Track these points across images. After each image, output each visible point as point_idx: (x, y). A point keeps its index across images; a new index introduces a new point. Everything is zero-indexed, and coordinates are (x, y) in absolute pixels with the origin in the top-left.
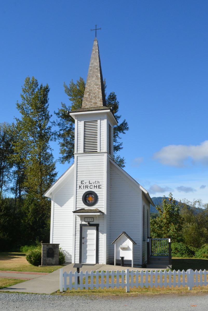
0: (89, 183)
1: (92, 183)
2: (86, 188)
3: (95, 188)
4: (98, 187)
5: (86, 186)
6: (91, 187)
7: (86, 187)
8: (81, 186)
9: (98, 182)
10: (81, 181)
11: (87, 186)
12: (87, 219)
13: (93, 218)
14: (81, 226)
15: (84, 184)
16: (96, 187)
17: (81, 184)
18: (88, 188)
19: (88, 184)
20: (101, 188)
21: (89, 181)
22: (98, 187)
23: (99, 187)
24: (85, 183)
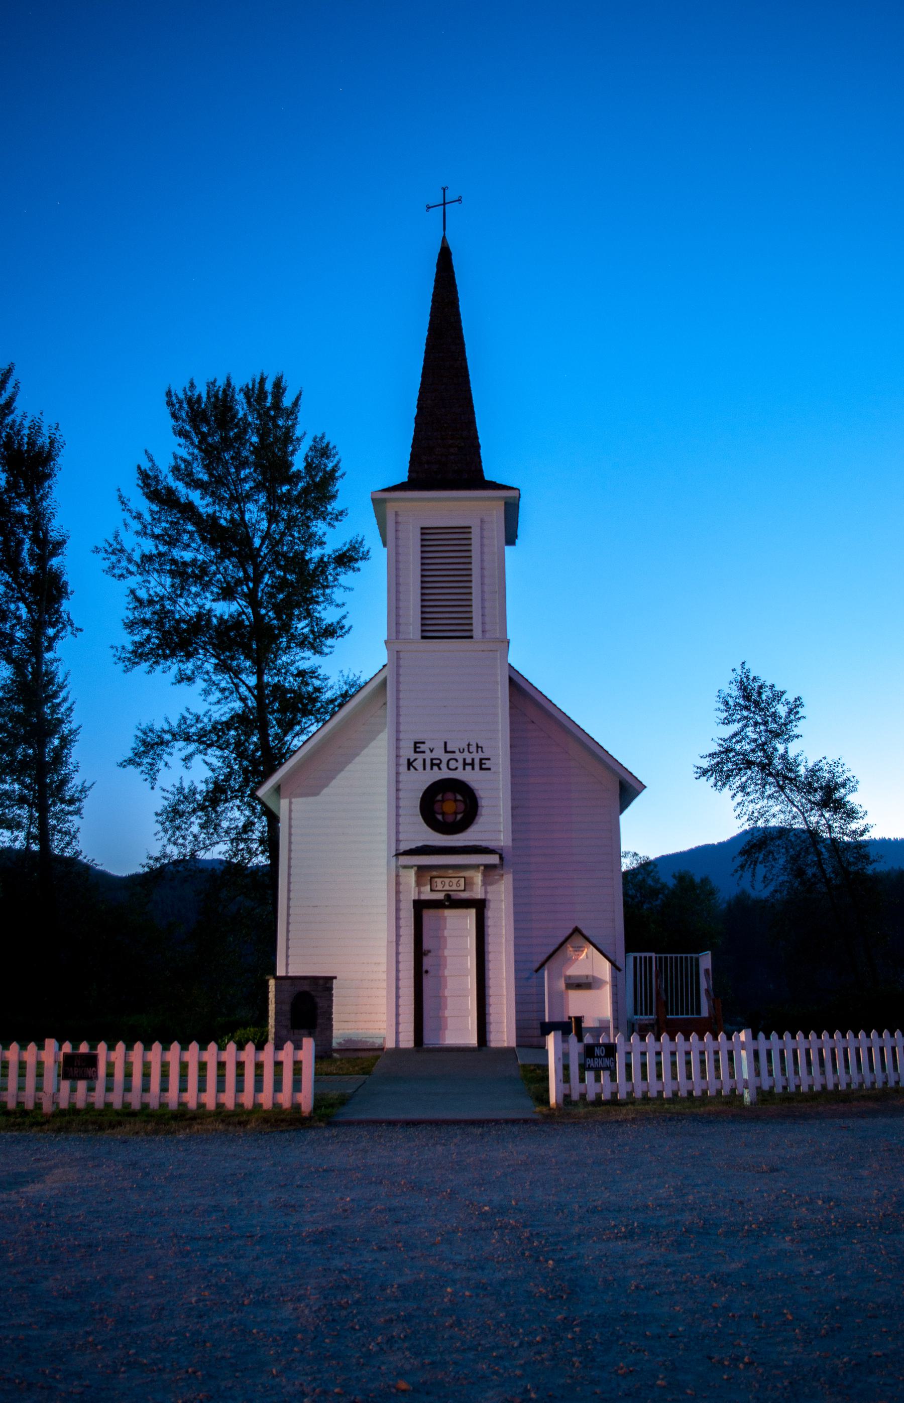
0: (446, 752)
1: (454, 752)
2: (432, 769)
3: (469, 768)
4: (477, 766)
5: (435, 762)
7: (432, 765)
8: (415, 760)
9: (478, 747)
10: (416, 743)
11: (438, 762)
14: (420, 906)
15: (424, 752)
17: (416, 752)
18: (440, 769)
19: (439, 753)
20: (489, 769)
21: (445, 743)
22: (477, 766)
23: (481, 764)
24: (428, 751)
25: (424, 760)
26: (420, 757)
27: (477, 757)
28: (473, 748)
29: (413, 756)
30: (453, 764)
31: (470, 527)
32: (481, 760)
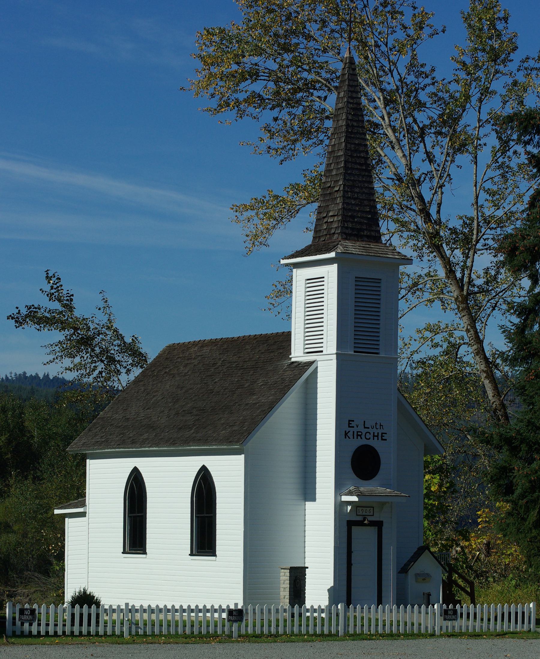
0: (365, 428)
1: (368, 428)
2: (357, 438)
3: (376, 438)
5: (359, 433)
6: (368, 438)
7: (358, 435)
8: (349, 432)
9: (380, 425)
10: (349, 421)
11: (360, 434)
12: (361, 509)
13: (373, 507)
15: (353, 427)
16: (377, 438)
17: (349, 427)
18: (361, 438)
19: (361, 428)
20: (386, 440)
21: (364, 422)
23: (382, 436)
24: (355, 427)
25: (354, 432)
26: (352, 430)
27: (380, 432)
28: (378, 426)
29: (348, 429)
30: (368, 436)
31: (380, 279)
32: (382, 433)
